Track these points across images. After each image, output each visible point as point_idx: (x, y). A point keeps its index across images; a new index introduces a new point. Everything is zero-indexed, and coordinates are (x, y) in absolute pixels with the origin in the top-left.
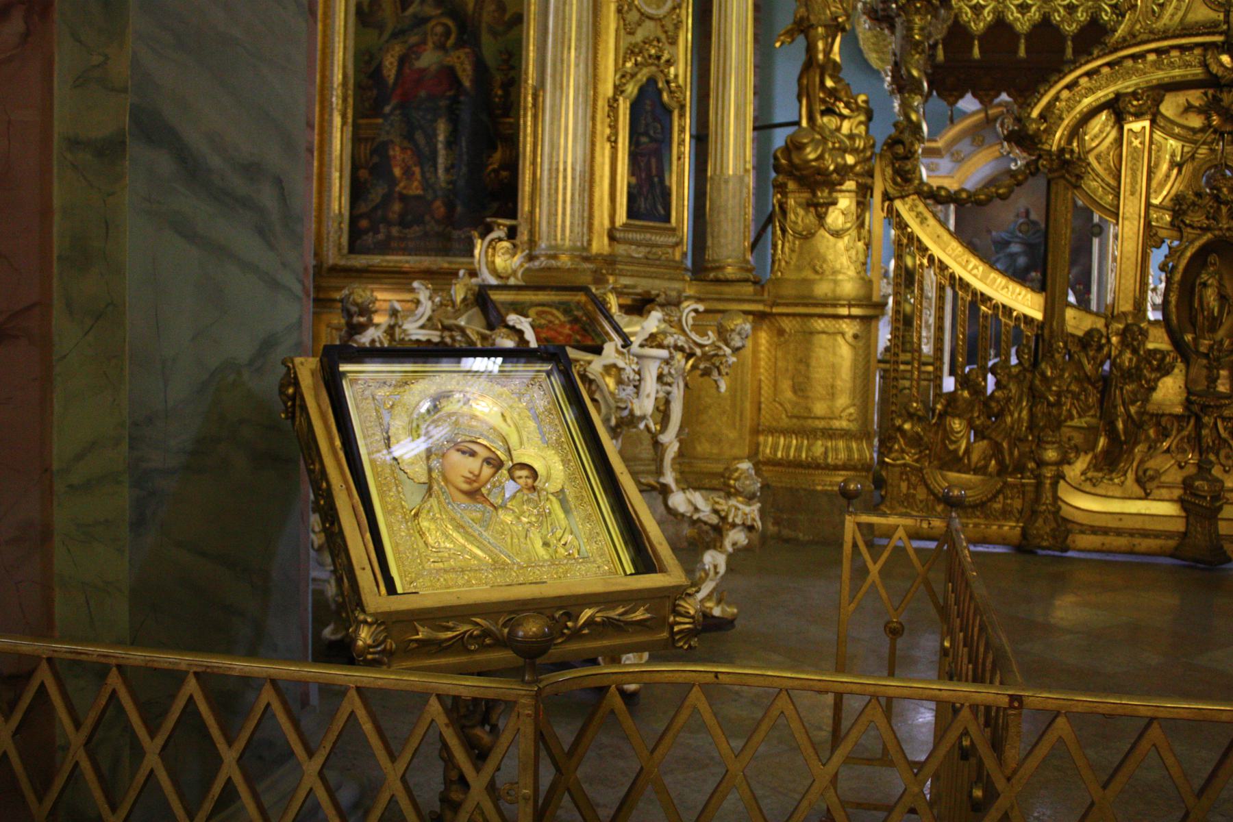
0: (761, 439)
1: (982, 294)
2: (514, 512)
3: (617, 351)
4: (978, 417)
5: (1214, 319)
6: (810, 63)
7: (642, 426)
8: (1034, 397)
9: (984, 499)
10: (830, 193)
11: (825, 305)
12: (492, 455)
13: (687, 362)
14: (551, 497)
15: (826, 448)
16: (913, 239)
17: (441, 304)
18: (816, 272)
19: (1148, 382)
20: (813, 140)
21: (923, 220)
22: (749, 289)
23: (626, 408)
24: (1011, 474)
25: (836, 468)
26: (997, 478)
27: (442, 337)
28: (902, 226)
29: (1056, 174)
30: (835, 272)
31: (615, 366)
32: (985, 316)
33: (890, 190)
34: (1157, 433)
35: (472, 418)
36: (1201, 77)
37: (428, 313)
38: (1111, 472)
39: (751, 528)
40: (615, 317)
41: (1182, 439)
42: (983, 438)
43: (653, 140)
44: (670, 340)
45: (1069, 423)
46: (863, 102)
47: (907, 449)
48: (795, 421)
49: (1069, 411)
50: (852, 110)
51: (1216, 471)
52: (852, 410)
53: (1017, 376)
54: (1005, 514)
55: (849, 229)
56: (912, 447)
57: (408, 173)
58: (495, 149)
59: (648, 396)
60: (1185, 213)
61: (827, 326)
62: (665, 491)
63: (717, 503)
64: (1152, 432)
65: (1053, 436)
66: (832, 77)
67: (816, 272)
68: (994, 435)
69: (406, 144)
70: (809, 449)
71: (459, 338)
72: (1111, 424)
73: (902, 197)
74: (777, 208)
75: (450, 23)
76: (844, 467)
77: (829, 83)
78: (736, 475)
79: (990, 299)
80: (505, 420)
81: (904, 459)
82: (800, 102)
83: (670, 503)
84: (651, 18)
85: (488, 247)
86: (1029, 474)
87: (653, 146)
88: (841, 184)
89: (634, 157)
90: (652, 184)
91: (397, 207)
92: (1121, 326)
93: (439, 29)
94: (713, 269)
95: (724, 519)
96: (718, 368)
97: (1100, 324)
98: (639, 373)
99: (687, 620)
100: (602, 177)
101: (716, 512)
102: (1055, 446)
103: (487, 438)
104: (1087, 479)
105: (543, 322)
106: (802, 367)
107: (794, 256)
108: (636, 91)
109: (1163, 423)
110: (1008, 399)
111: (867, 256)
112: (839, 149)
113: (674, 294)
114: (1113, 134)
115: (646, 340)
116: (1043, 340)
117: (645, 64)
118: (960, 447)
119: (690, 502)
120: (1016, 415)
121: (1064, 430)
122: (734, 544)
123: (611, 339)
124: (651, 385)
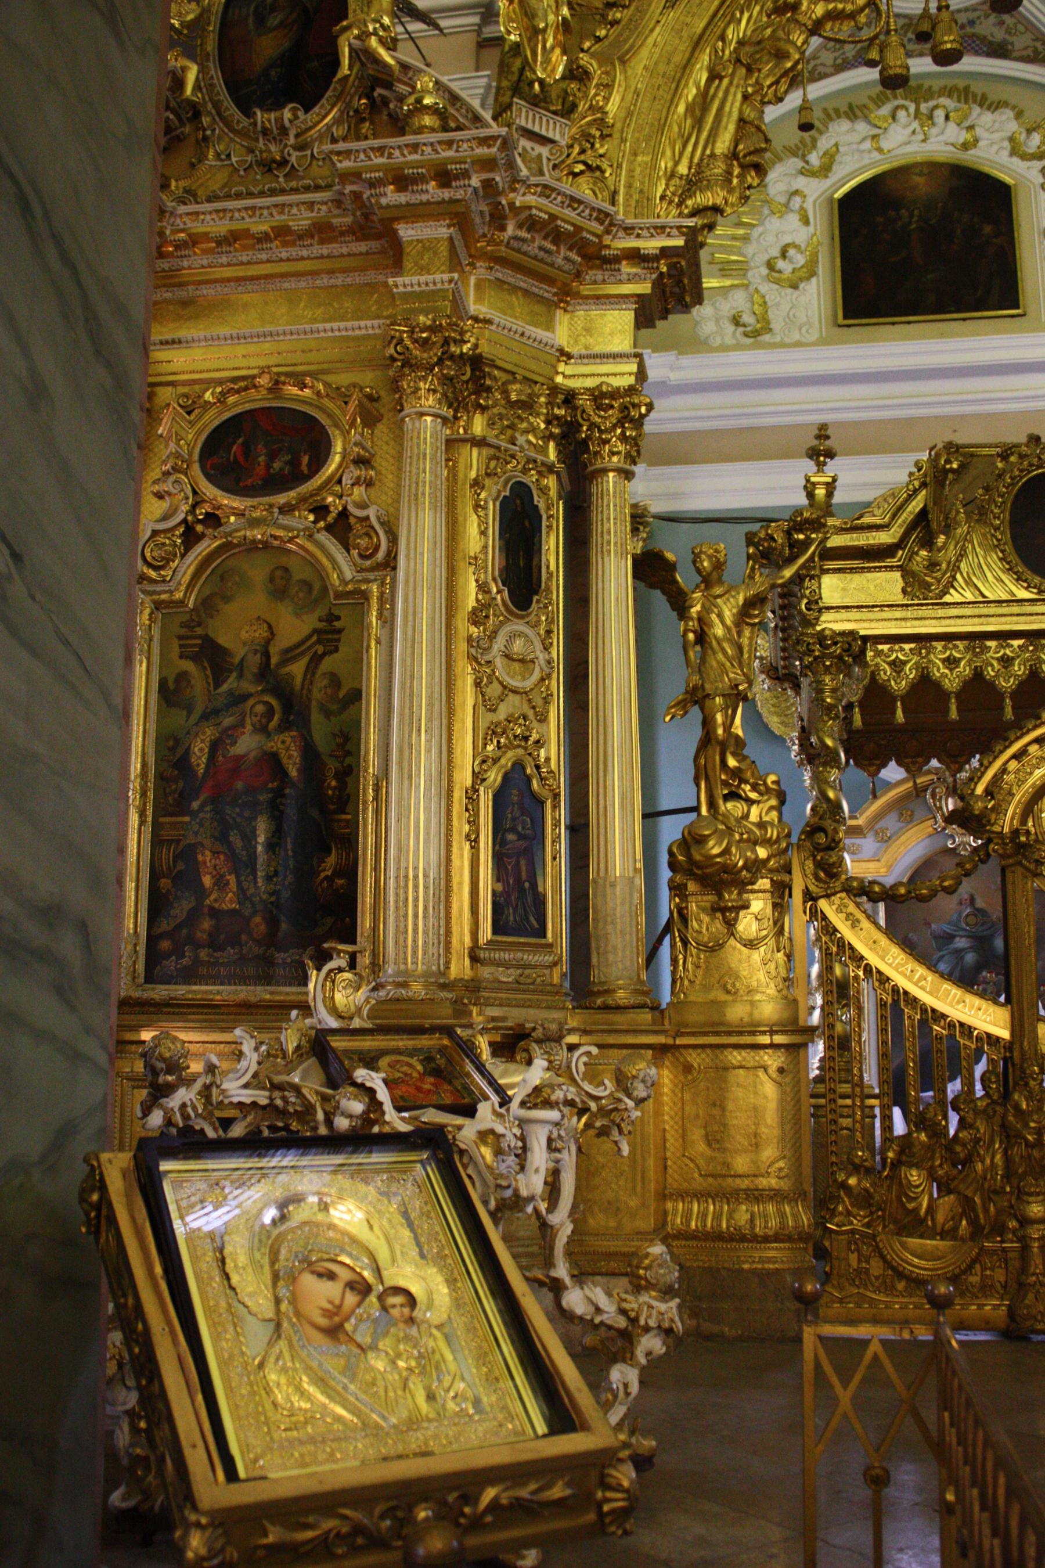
0: (669, 1205)
1: (933, 1010)
2: (387, 1353)
3: (495, 1112)
4: (941, 1165)
6: (707, 740)
7: (529, 1209)
8: (1008, 1137)
9: (957, 1271)
10: (740, 894)
11: (741, 1033)
12: (357, 1278)
13: (579, 1120)
14: (435, 1331)
15: (752, 1215)
16: (844, 946)
17: (269, 1055)
18: (728, 992)
20: (715, 832)
21: (855, 924)
22: (646, 1016)
23: (509, 1187)
24: (987, 1238)
25: (766, 1239)
26: (971, 1243)
27: (271, 1099)
28: (829, 929)
29: (1011, 861)
30: (750, 992)
31: (492, 1131)
32: (939, 1038)
33: (812, 888)
35: (329, 1228)
37: (254, 1067)
39: (669, 1332)
40: (487, 1066)
42: (950, 1192)
43: (521, 837)
44: (558, 1095)
46: (773, 782)
47: (854, 1211)
48: (710, 1180)
50: (761, 794)
52: (781, 1164)
53: (984, 1111)
54: (986, 1289)
55: (766, 937)
56: (860, 1208)
57: (220, 883)
58: (329, 852)
59: (537, 1171)
61: (744, 1059)
62: (557, 1287)
63: (625, 1300)
65: (1038, 1186)
66: (734, 754)
67: (728, 992)
68: (961, 1187)
69: (218, 847)
70: (730, 1217)
71: (293, 1100)
73: (828, 896)
74: (675, 915)
75: (274, 702)
76: (776, 1238)
77: (732, 762)
78: (647, 1262)
79: (944, 1016)
80: (371, 1227)
81: (851, 1223)
82: (698, 785)
83: (564, 1303)
84: (515, 692)
85: (325, 980)
86: (1010, 1236)
87: (522, 844)
88: (753, 883)
89: (499, 858)
90: (522, 891)
91: (206, 924)
93: (260, 709)
94: (600, 993)
95: (634, 1321)
96: (619, 1126)
98: (523, 1138)
99: (619, 1495)
100: (460, 884)
101: (623, 1312)
102: (1041, 1198)
103: (350, 1255)
105: (398, 1075)
106: (716, 1112)
107: (700, 973)
108: (499, 779)
110: (977, 1141)
111: (789, 970)
112: (748, 840)
113: (554, 1027)
115: (529, 1096)
116: (1013, 1065)
117: (510, 747)
118: (921, 1205)
119: (589, 1300)
120: (988, 1161)
122: (648, 1354)
123: (486, 1098)
124: (539, 1158)
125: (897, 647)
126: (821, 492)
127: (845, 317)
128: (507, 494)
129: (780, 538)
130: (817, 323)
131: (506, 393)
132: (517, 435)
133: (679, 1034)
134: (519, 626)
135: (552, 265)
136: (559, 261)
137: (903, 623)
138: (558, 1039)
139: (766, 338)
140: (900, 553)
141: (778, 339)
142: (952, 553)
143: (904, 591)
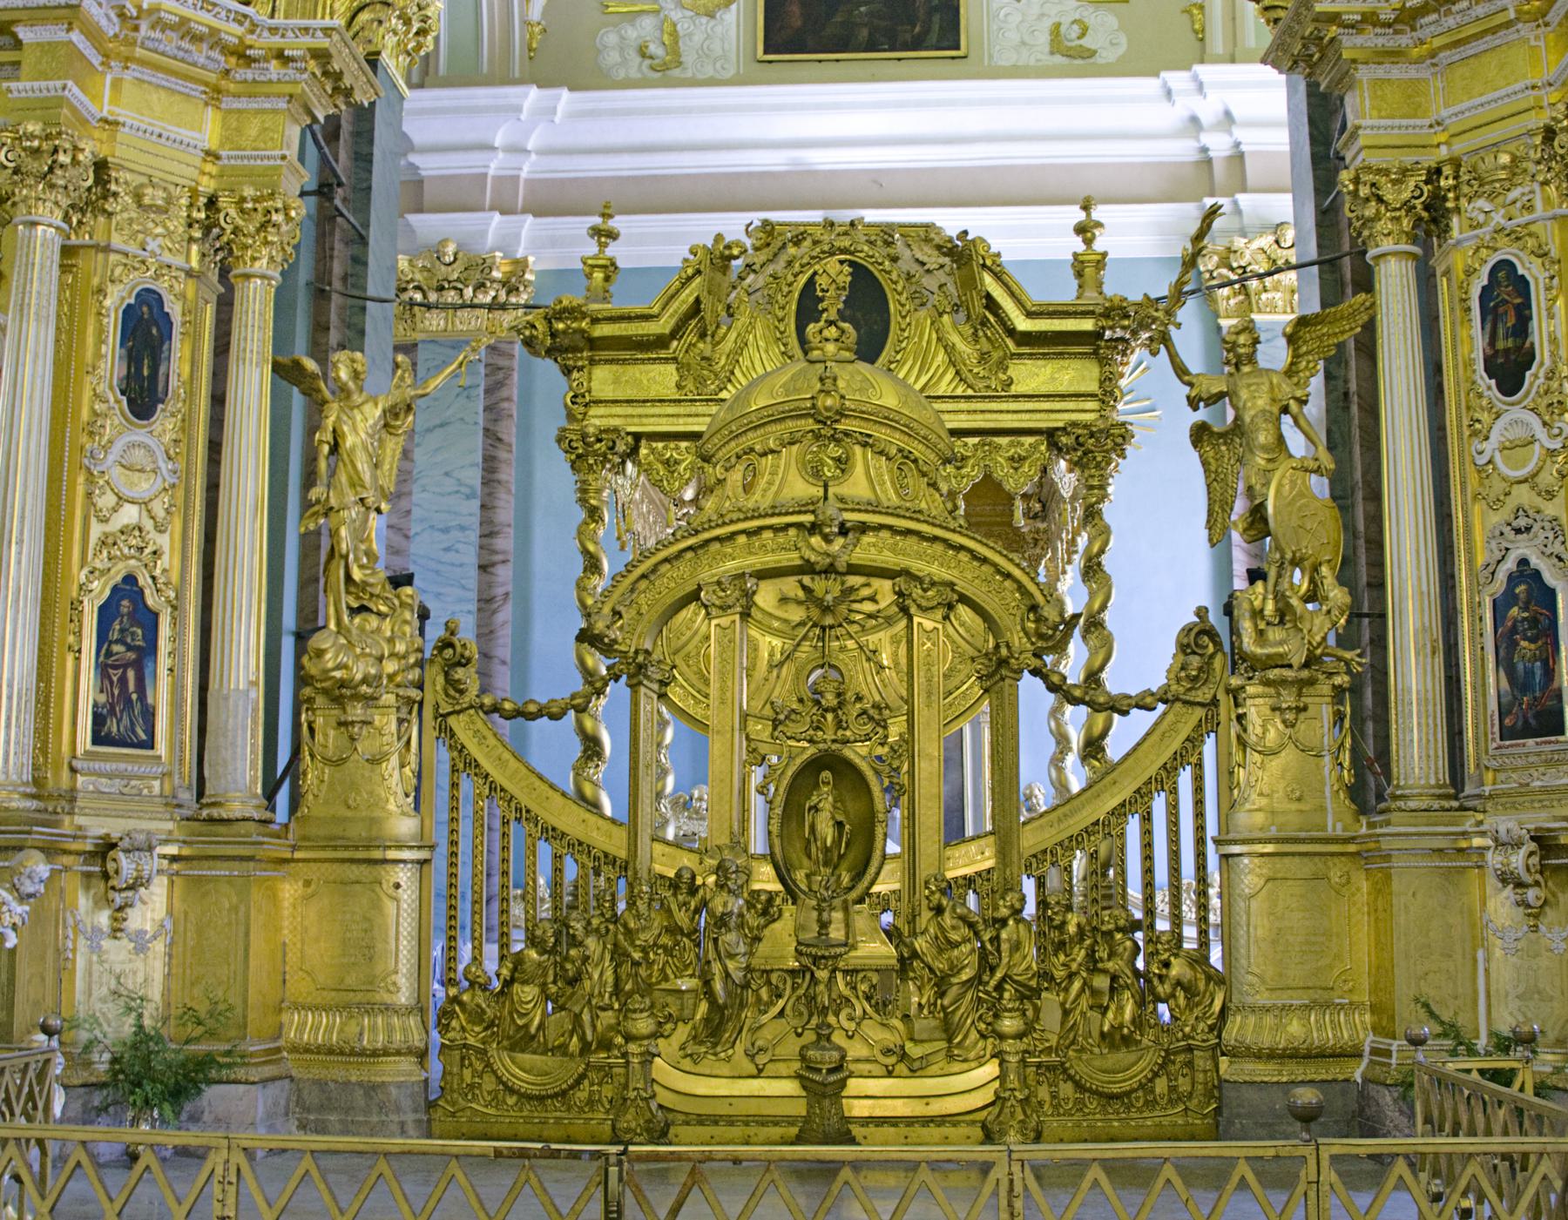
0: (285, 1017)
5: (827, 850)
11: (356, 848)
19: (751, 930)
34: (770, 991)
36: (799, 562)
38: (715, 1045)
41: (799, 998)
42: (562, 1008)
43: (129, 648)
45: (664, 986)
47: (469, 1027)
49: (663, 970)
51: (838, 1038)
53: (597, 930)
56: (474, 1023)
60: (781, 722)
64: (764, 993)
70: (341, 1031)
72: (707, 983)
87: (132, 656)
89: (103, 669)
92: (714, 862)
97: (688, 860)
104: (686, 1056)
107: (324, 787)
109: (774, 981)
114: (704, 628)
118: (532, 1020)
121: (656, 994)
125: (672, 445)
126: (599, 275)
127: (766, 52)
128: (132, 301)
129: (541, 326)
130: (734, 58)
131: (138, 197)
132: (149, 239)
133: (294, 848)
134: (139, 434)
135: (194, 64)
136: (202, 60)
137: (675, 420)
138: (150, 849)
139: (676, 72)
140: (675, 343)
141: (689, 74)
142: (729, 345)
143: (679, 387)
